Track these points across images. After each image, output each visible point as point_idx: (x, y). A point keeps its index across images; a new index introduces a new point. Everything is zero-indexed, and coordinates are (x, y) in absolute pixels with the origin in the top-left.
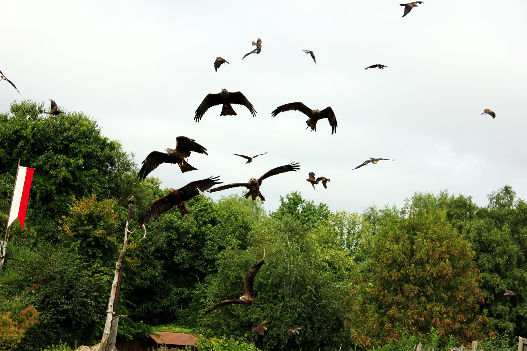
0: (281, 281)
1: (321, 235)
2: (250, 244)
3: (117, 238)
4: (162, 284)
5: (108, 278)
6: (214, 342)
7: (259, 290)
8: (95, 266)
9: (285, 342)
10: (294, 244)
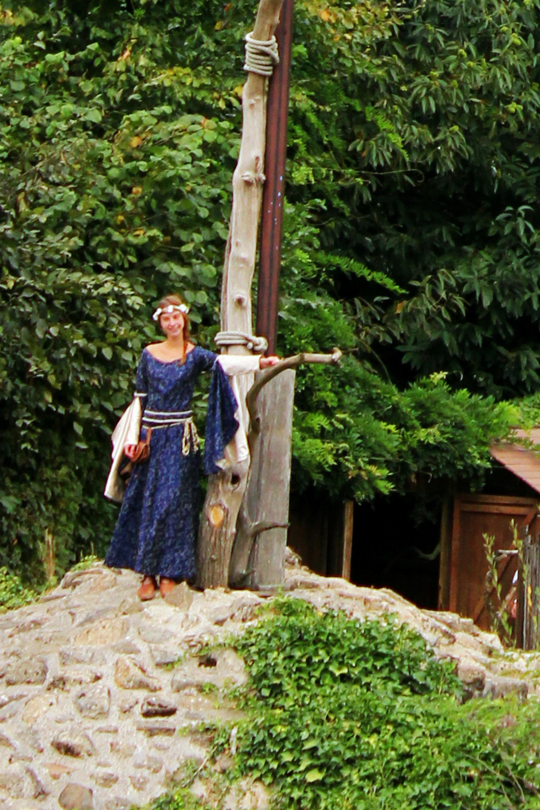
8: (119, 66)
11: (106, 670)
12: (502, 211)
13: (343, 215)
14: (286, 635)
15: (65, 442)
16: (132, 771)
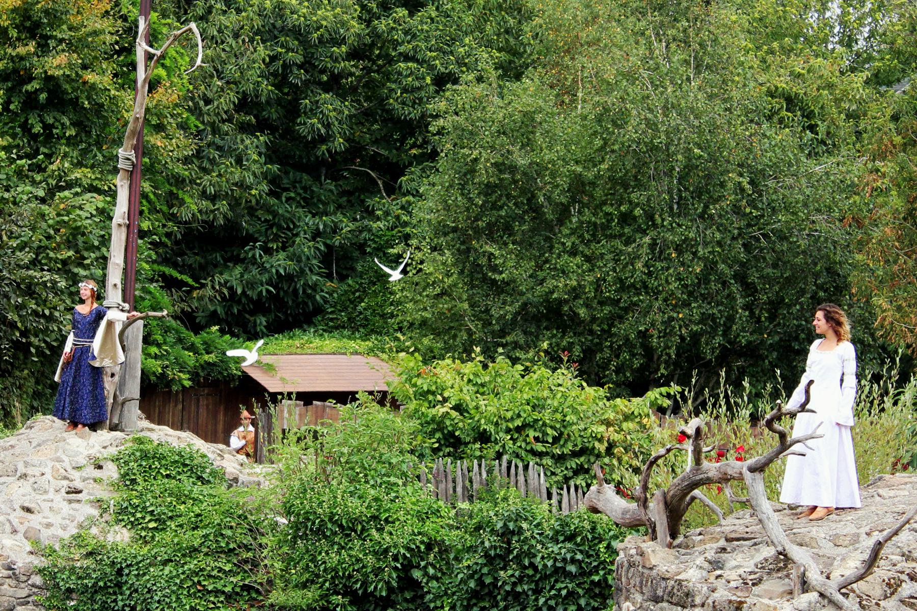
0: (641, 164)
1: (756, 15)
2: (534, 61)
3: (116, 75)
4: (269, 209)
5: (99, 201)
6: (443, 372)
7: (574, 200)
8: (54, 167)
9: (669, 355)
10: (673, 46)
11: (48, 470)
12: (248, 245)
13: (167, 246)
14: (138, 454)
15: (26, 358)
16: (60, 521)
